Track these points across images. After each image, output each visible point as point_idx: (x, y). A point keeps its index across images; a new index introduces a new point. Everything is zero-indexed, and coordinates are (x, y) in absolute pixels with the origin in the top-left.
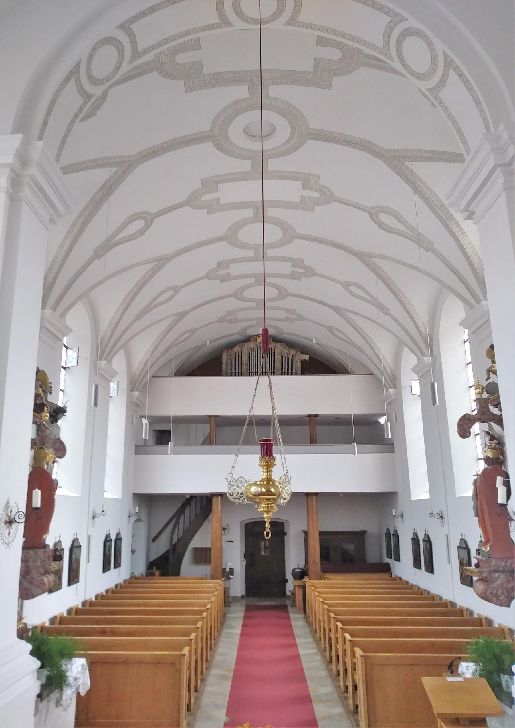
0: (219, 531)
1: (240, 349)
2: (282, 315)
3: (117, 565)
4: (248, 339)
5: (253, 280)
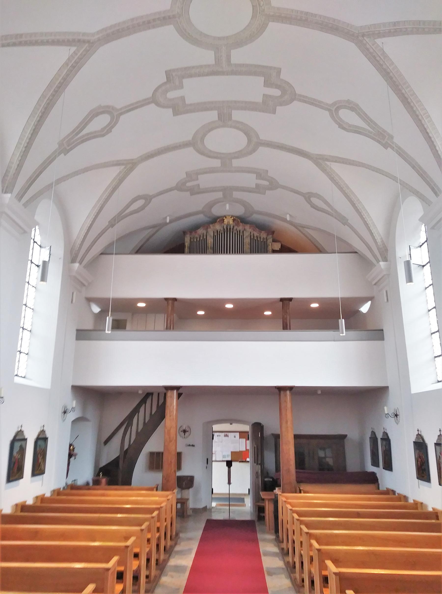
0: (173, 431)
2: (250, 180)
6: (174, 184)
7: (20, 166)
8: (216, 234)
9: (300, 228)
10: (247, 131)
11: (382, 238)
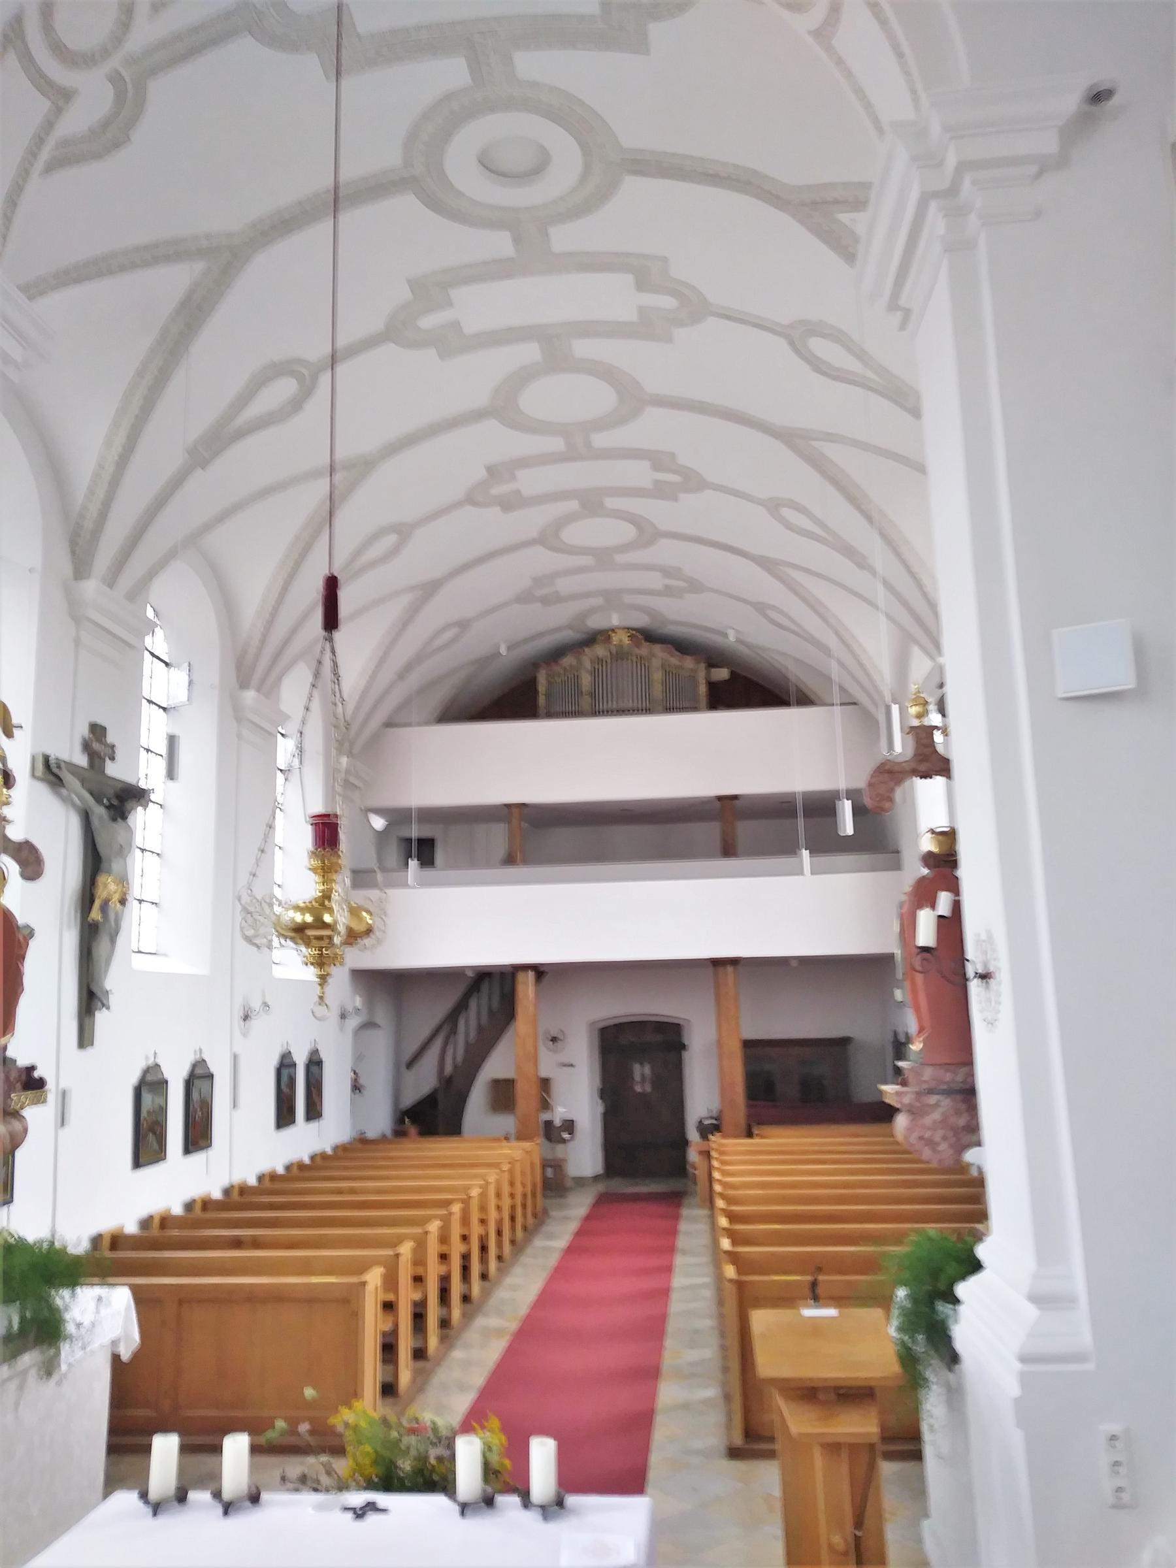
3: (314, 1112)
4: (593, 638)
5: (574, 505)
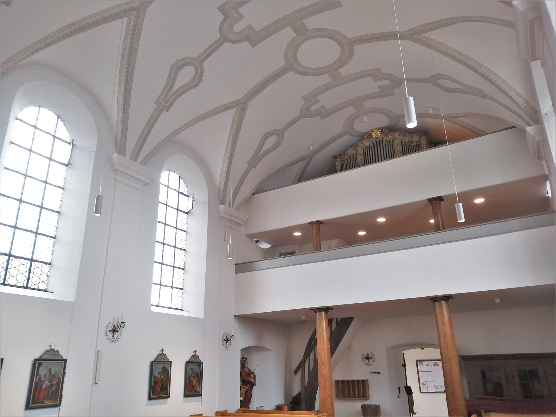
1: (354, 151)
2: (370, 86)
6: (298, 113)
7: (125, 130)
8: (365, 151)
9: (453, 120)
10: (332, 35)
11: (524, 99)
